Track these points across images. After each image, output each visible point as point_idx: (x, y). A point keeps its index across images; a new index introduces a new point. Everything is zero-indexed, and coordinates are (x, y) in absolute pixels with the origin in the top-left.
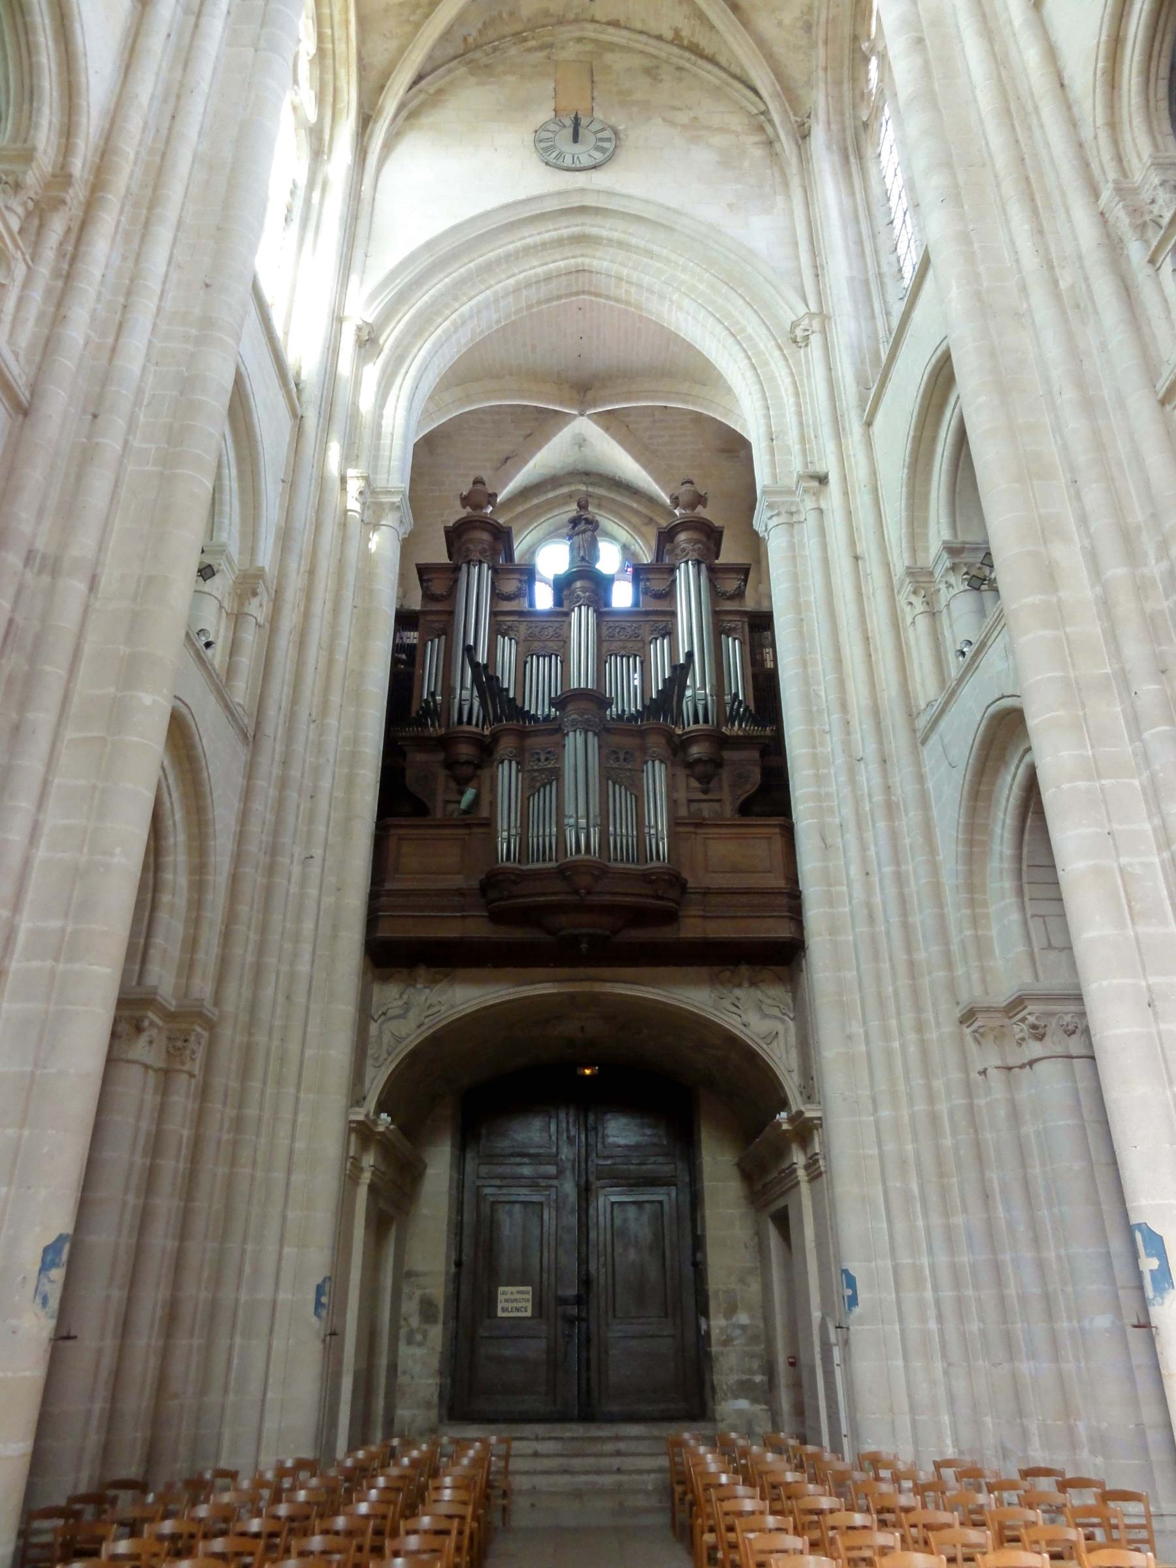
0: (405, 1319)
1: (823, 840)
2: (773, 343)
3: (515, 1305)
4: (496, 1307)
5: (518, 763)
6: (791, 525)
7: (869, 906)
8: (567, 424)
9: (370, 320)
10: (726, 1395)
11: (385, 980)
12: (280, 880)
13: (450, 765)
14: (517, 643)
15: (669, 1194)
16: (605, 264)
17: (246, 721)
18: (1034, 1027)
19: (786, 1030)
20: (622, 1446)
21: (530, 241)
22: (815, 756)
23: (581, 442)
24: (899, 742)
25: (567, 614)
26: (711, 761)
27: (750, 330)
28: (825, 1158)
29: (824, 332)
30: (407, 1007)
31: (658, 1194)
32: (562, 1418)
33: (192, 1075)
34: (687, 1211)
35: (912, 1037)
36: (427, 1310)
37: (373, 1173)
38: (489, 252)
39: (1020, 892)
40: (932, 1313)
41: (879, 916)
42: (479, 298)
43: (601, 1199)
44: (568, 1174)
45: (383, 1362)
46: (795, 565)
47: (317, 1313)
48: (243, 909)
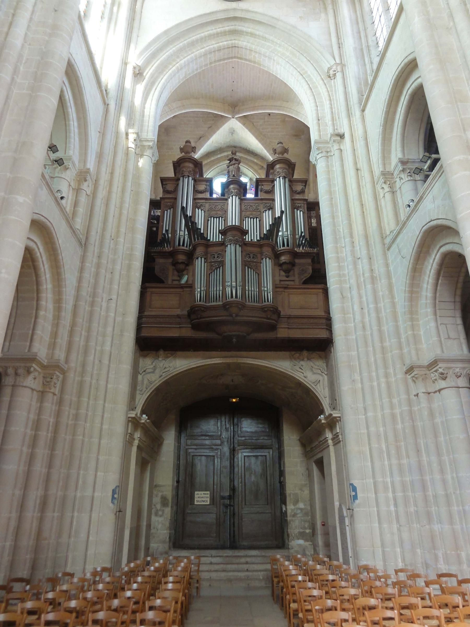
0: (154, 505)
1: (342, 294)
2: (319, 77)
3: (202, 499)
5: (205, 259)
6: (328, 157)
7: (363, 322)
8: (226, 122)
9: (140, 64)
10: (294, 538)
11: (145, 356)
12: (97, 309)
13: (175, 264)
14: (204, 212)
15: (269, 453)
16: (245, 43)
17: (81, 236)
18: (442, 374)
19: (323, 379)
20: (249, 560)
21: (211, 32)
22: (338, 257)
23: (232, 132)
24: (377, 249)
25: (227, 200)
26: (290, 263)
27: (309, 73)
28: (342, 435)
29: (342, 72)
30: (155, 368)
31: (265, 452)
32: (223, 547)
33: (54, 394)
34: (277, 460)
35: (383, 380)
37: (139, 441)
38: (193, 36)
39: (435, 314)
40: (392, 502)
41: (368, 327)
42: (189, 57)
43: (240, 455)
44: (226, 443)
45: (144, 524)
46: (329, 175)
47: (112, 502)
48: (79, 320)
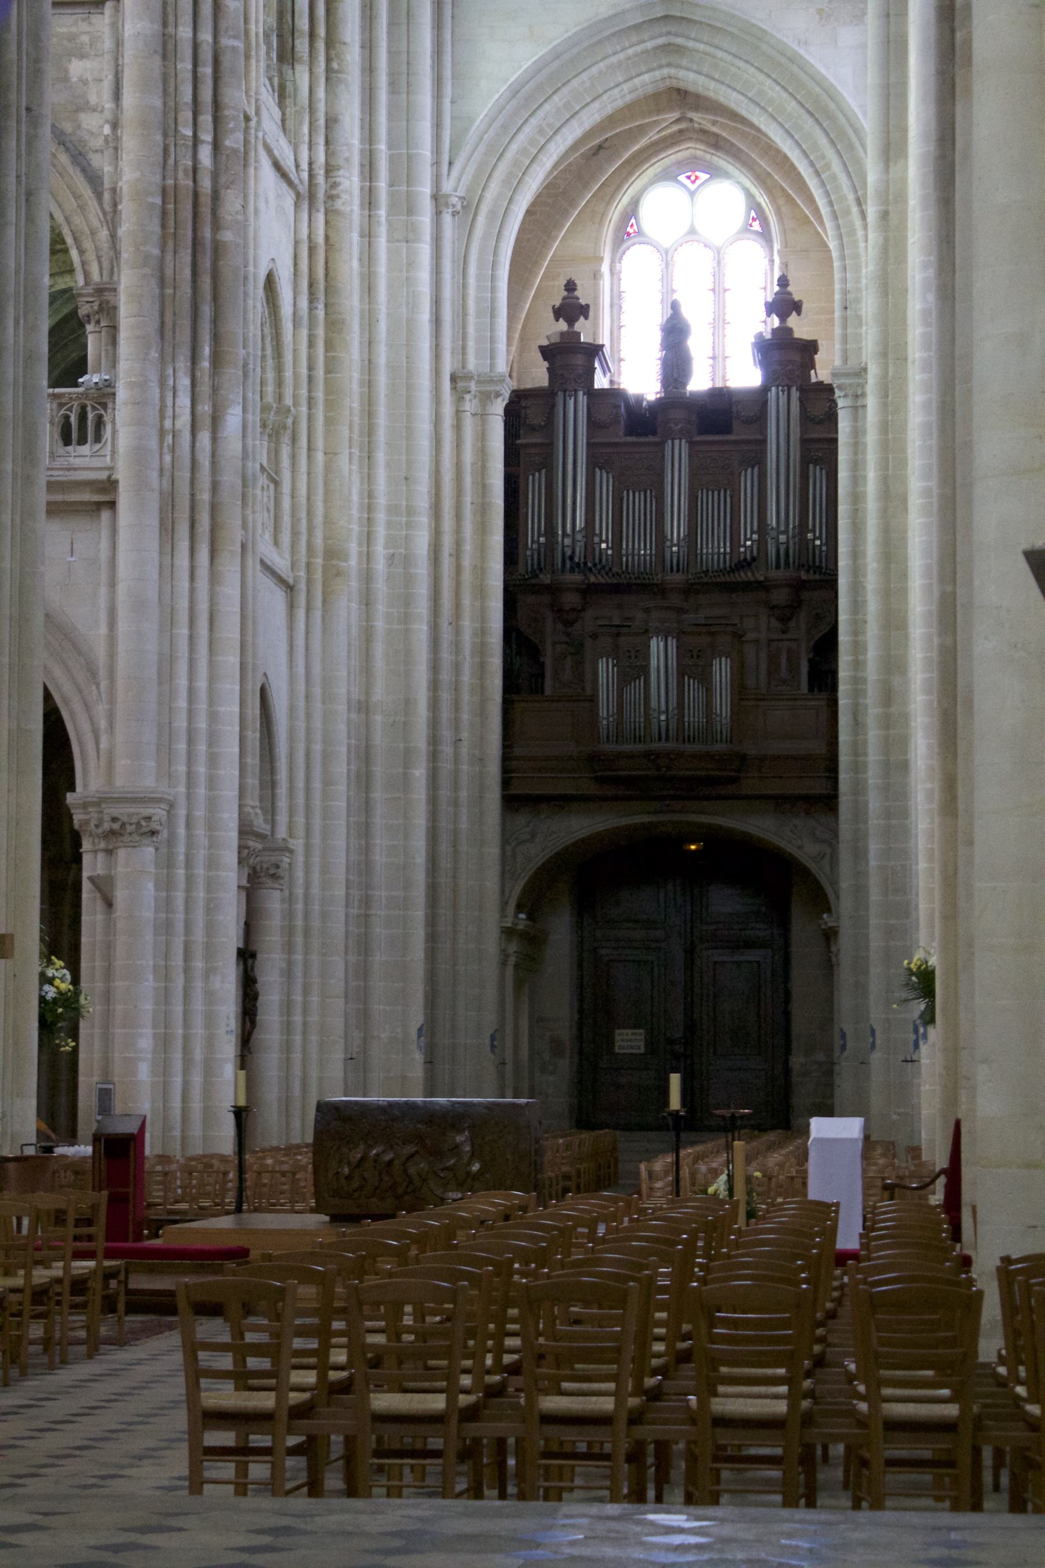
4: (613, 1044)
13: (558, 611)
25: (661, 444)
30: (533, 835)
31: (754, 955)
36: (557, 1049)
47: (492, 1051)
